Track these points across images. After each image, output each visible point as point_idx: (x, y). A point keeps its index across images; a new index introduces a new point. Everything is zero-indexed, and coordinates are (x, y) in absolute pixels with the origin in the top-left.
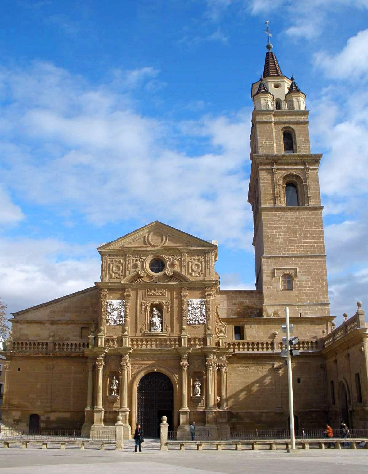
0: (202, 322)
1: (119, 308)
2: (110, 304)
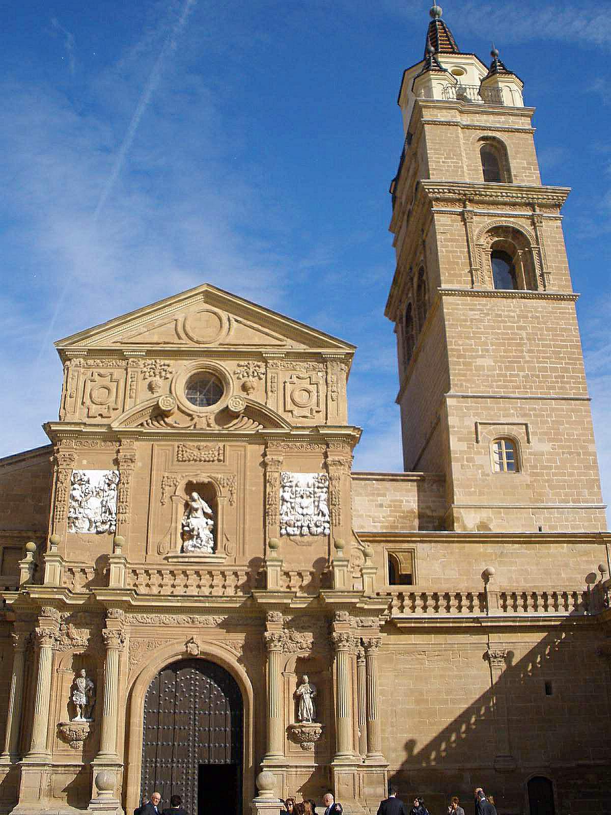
0: (320, 530)
1: (103, 490)
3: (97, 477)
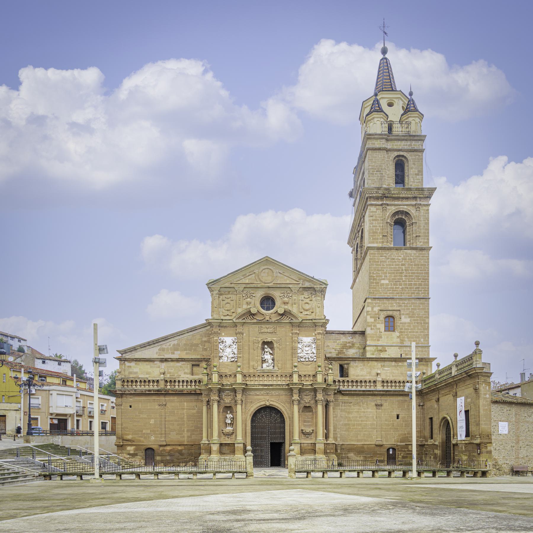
0: (312, 359)
2: (222, 341)
3: (229, 340)
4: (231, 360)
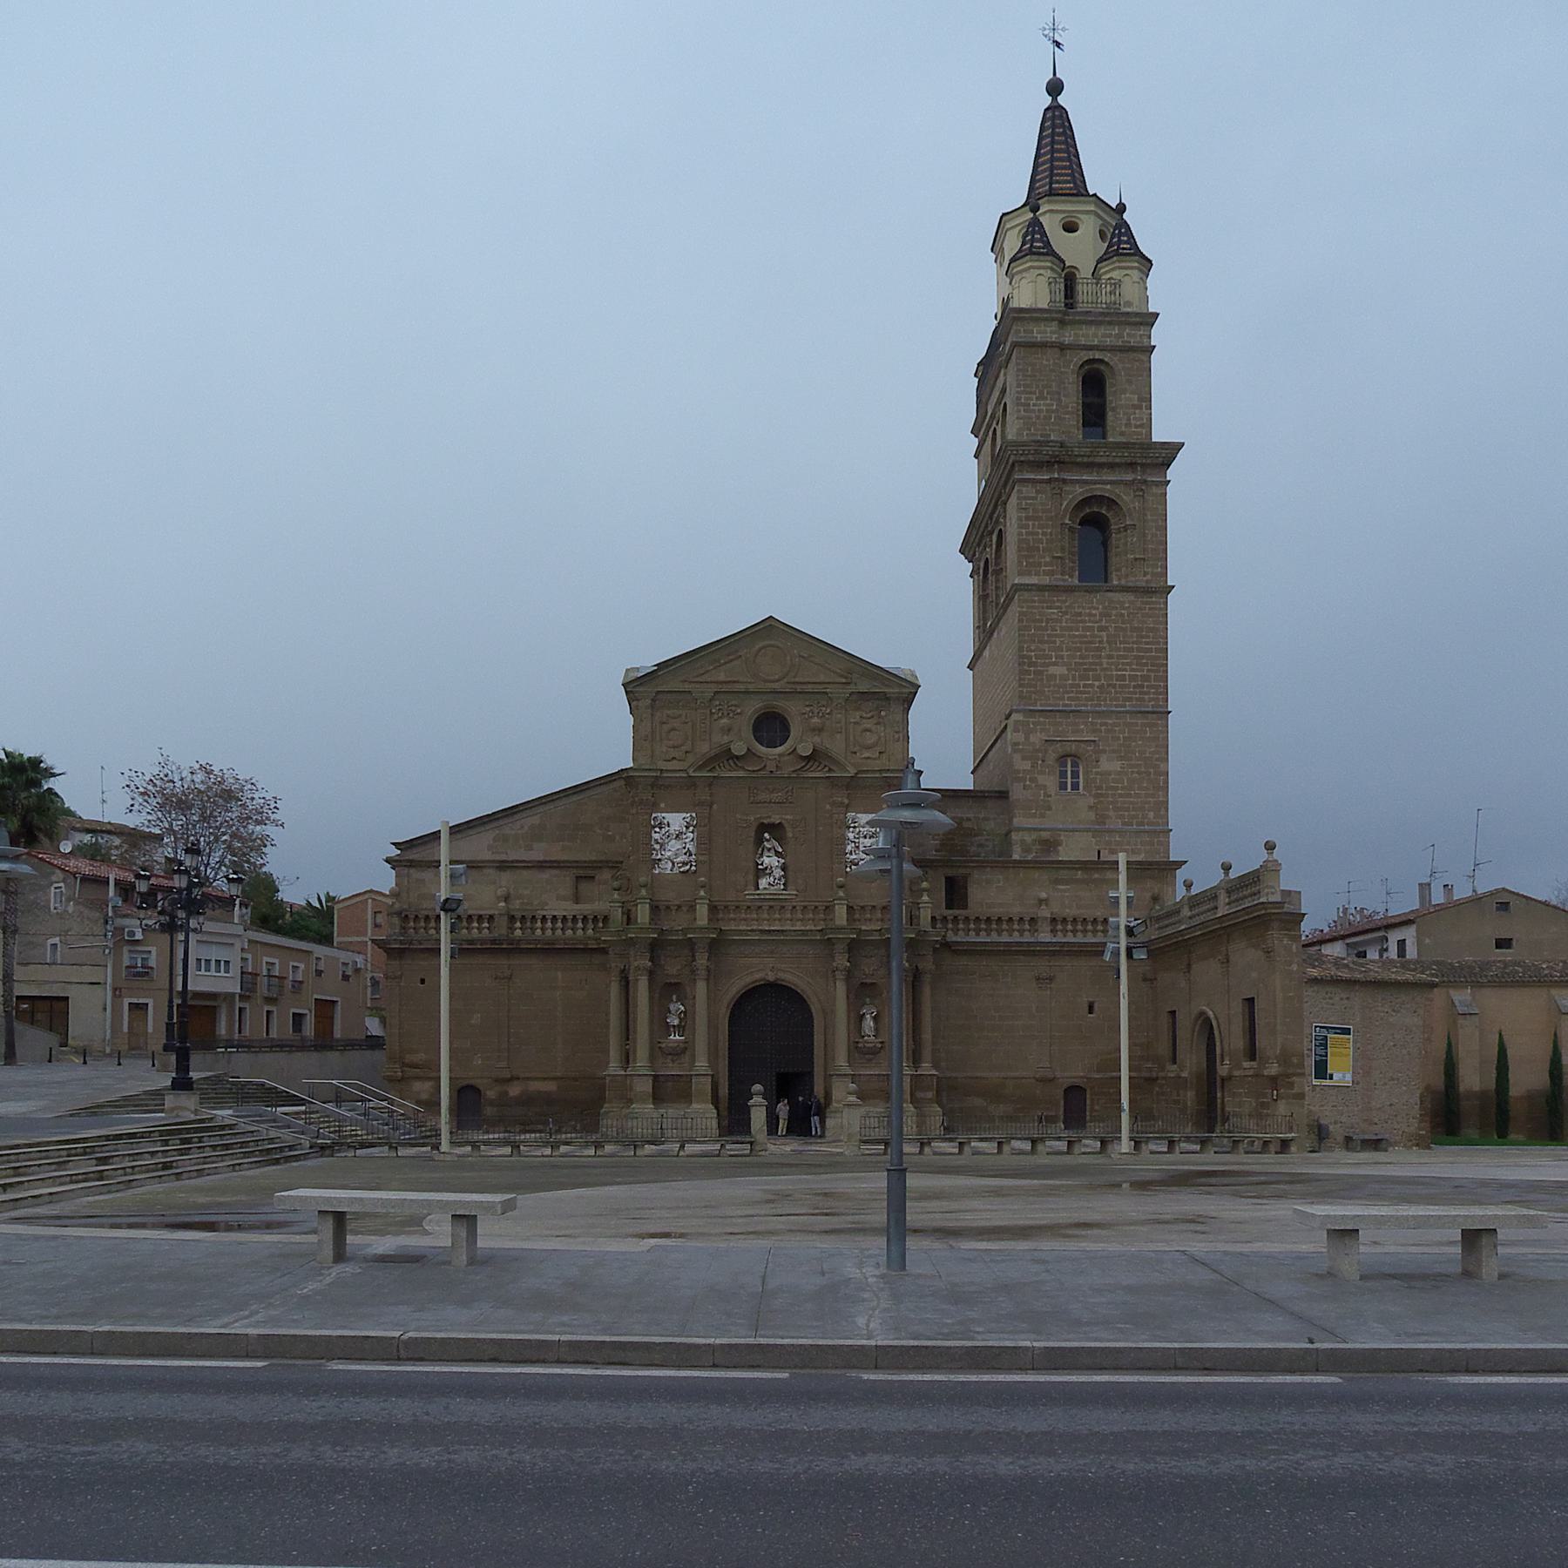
2: (660, 823)
4: (681, 870)
